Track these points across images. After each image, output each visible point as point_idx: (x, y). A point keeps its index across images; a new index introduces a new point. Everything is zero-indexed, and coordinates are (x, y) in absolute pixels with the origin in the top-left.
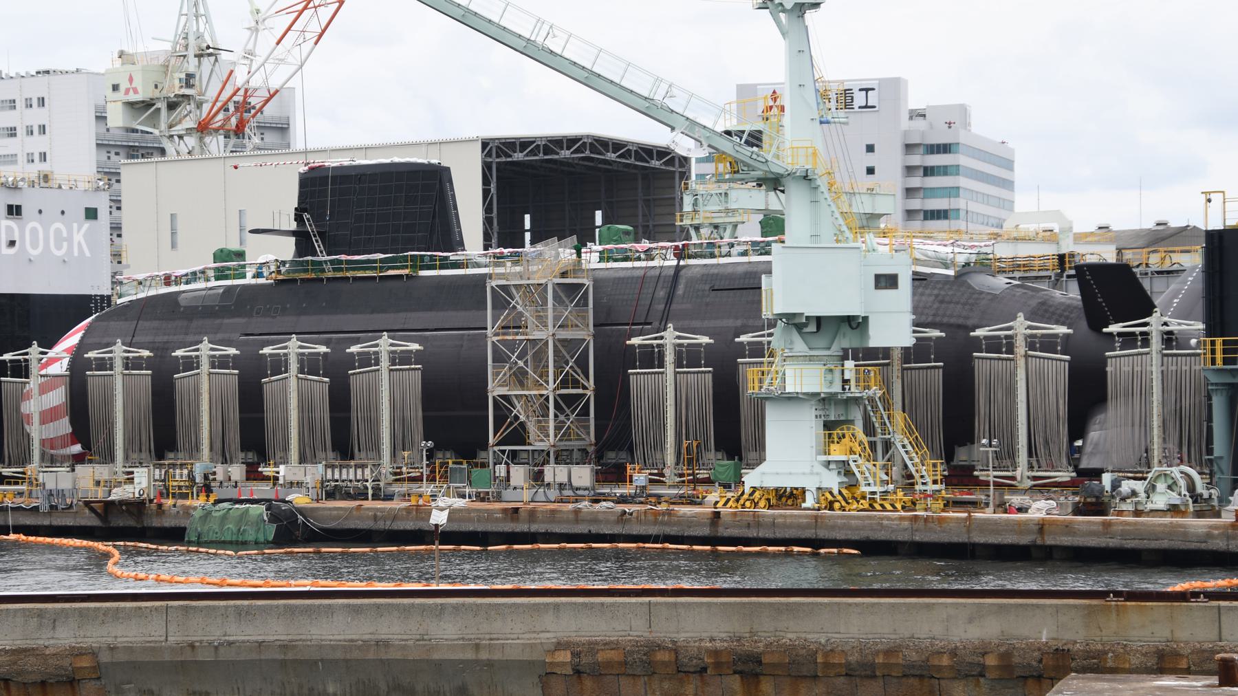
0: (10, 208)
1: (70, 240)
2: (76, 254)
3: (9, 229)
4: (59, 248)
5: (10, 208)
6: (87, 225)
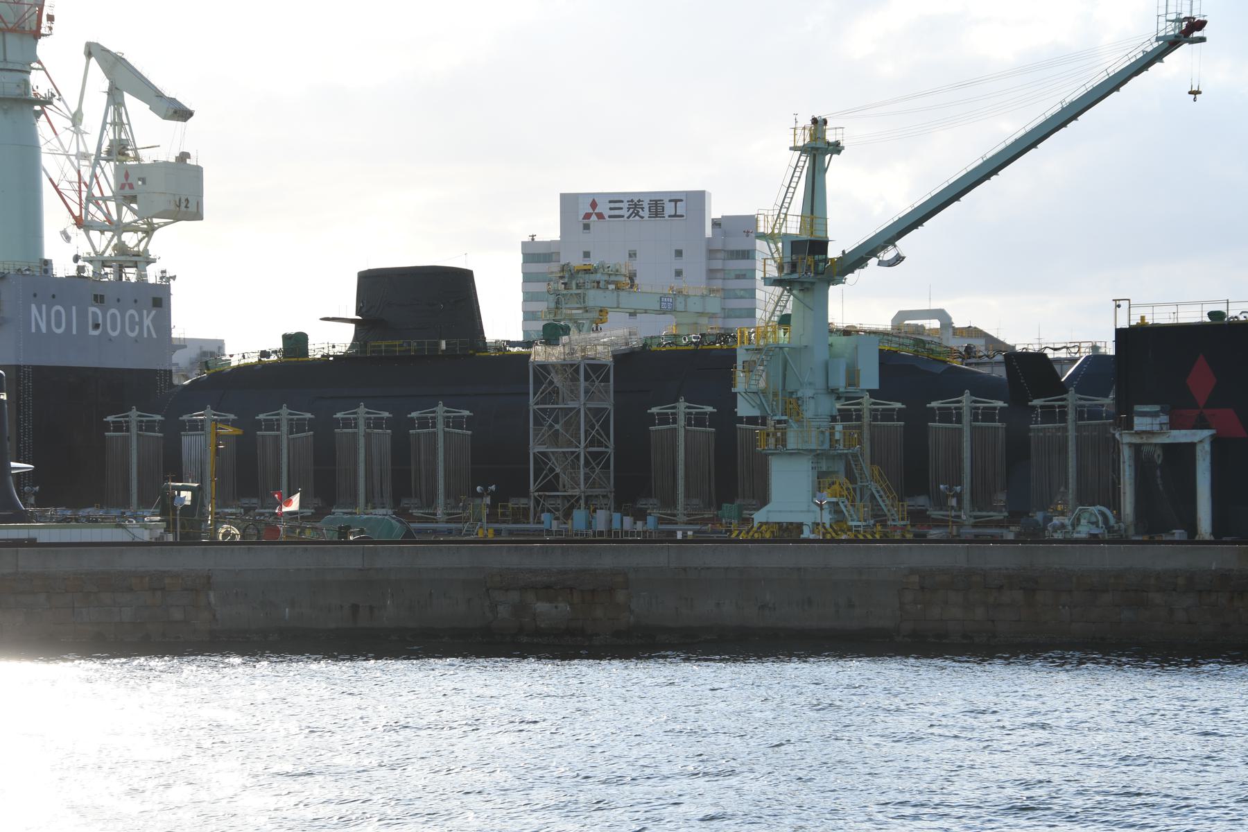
0: (96, 297)
3: (94, 314)
4: (132, 330)
5: (96, 297)
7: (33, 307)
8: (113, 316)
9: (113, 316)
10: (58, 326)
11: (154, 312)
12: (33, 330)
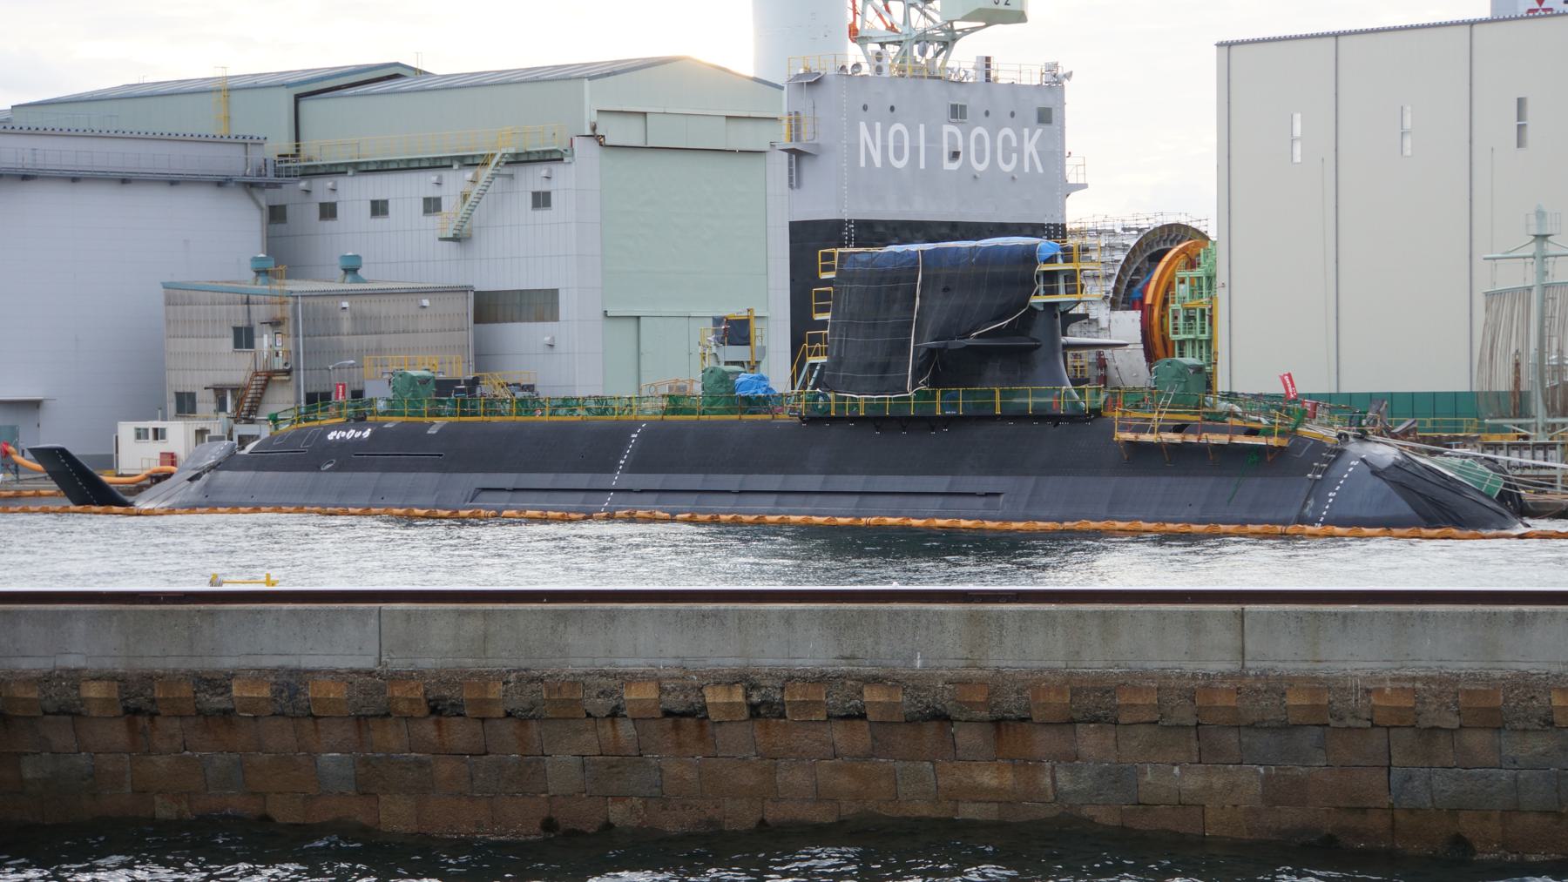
0: (954, 108)
1: (1020, 151)
2: (1027, 169)
3: (951, 135)
4: (1007, 161)
5: (954, 108)
6: (1039, 131)
7: (863, 125)
8: (980, 138)
9: (980, 138)
10: (899, 156)
11: (1039, 131)
12: (863, 164)
